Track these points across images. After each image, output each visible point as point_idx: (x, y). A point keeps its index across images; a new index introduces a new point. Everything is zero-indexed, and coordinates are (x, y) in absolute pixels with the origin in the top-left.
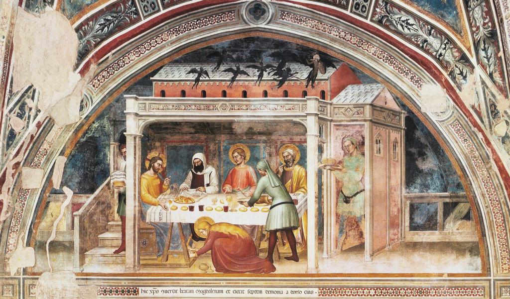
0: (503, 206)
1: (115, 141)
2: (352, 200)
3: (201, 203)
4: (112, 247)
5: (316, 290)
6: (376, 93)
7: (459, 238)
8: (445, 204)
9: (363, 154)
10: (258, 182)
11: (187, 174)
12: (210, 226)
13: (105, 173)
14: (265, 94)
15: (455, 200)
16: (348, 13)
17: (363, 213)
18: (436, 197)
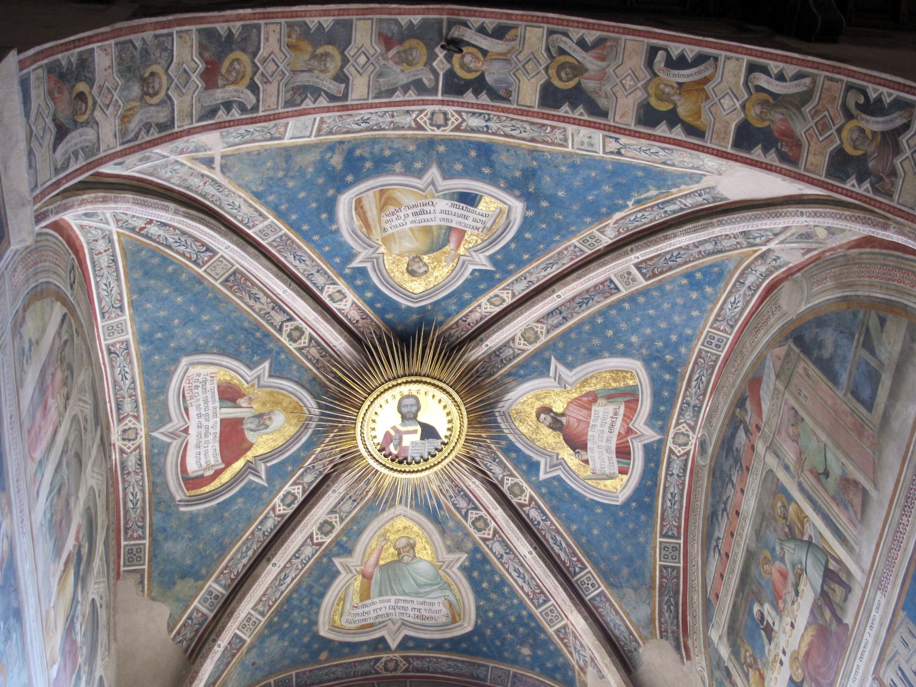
0: (887, 263)
2: (829, 469)
5: (879, 593)
6: (771, 364)
7: (898, 348)
8: (864, 346)
9: (803, 420)
11: (760, 635)
12: (796, 658)
14: (742, 491)
15: (864, 330)
16: (723, 355)
18: (855, 355)
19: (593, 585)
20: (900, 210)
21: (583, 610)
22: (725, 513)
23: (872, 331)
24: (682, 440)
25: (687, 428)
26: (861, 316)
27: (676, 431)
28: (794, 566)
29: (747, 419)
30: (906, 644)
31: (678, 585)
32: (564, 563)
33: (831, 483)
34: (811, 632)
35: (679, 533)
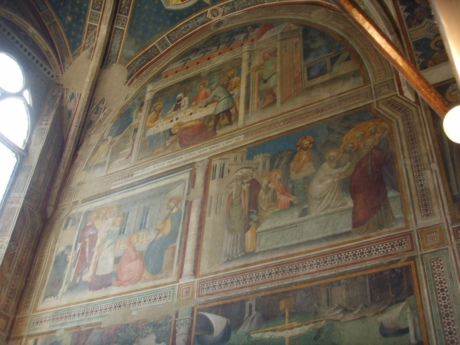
1: (138, 106)
2: (268, 81)
3: (177, 117)
4: (125, 156)
5: (243, 136)
6: (284, 27)
7: (344, 72)
8: (331, 59)
9: (276, 56)
10: (211, 93)
11: (172, 106)
12: (180, 125)
13: (130, 122)
14: (220, 54)
16: (266, 4)
17: (275, 84)
18: (325, 57)
19: (123, 24)
20: (407, 35)
21: (110, 29)
22: (203, 54)
23: (340, 59)
24: (215, 13)
25: (222, 11)
26: (342, 49)
27: (217, 8)
28: (215, 96)
29: (251, 34)
30: (236, 159)
31: (153, 58)
32: (121, 5)
33: (263, 86)
34: (198, 123)
35: (174, 42)
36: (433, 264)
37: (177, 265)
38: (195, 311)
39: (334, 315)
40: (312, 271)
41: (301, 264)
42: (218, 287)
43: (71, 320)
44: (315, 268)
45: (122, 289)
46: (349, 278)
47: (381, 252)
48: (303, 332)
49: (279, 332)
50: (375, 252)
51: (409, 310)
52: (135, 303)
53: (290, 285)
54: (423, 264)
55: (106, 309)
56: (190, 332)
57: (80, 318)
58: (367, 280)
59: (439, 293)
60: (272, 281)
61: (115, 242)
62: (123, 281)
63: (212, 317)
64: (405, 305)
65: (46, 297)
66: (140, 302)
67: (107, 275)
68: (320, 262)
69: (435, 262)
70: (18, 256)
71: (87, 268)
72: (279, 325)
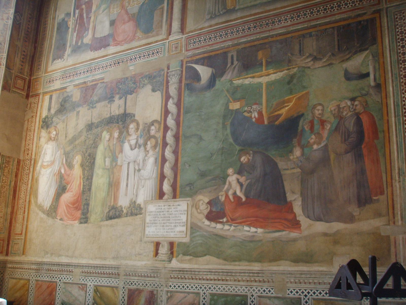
36: (396, 17)
37: (166, 25)
38: (184, 63)
39: (305, 63)
40: (286, 24)
41: (276, 19)
42: (203, 41)
43: (79, 77)
44: (289, 22)
45: (119, 48)
46: (320, 30)
47: (350, 6)
48: (278, 78)
49: (257, 79)
50: (344, 6)
51: (371, 57)
52: (131, 59)
53: (267, 38)
54: (387, 17)
55: (107, 66)
56: (180, 81)
57: (86, 75)
58: (336, 32)
59: (399, 42)
60: (250, 35)
61: (109, 7)
62: (119, 41)
63: (199, 68)
64: (367, 53)
65: (54, 60)
66: (136, 58)
67: (105, 37)
68: (294, 16)
69: (398, 15)
70: (24, 26)
71: (87, 32)
72: (257, 72)
